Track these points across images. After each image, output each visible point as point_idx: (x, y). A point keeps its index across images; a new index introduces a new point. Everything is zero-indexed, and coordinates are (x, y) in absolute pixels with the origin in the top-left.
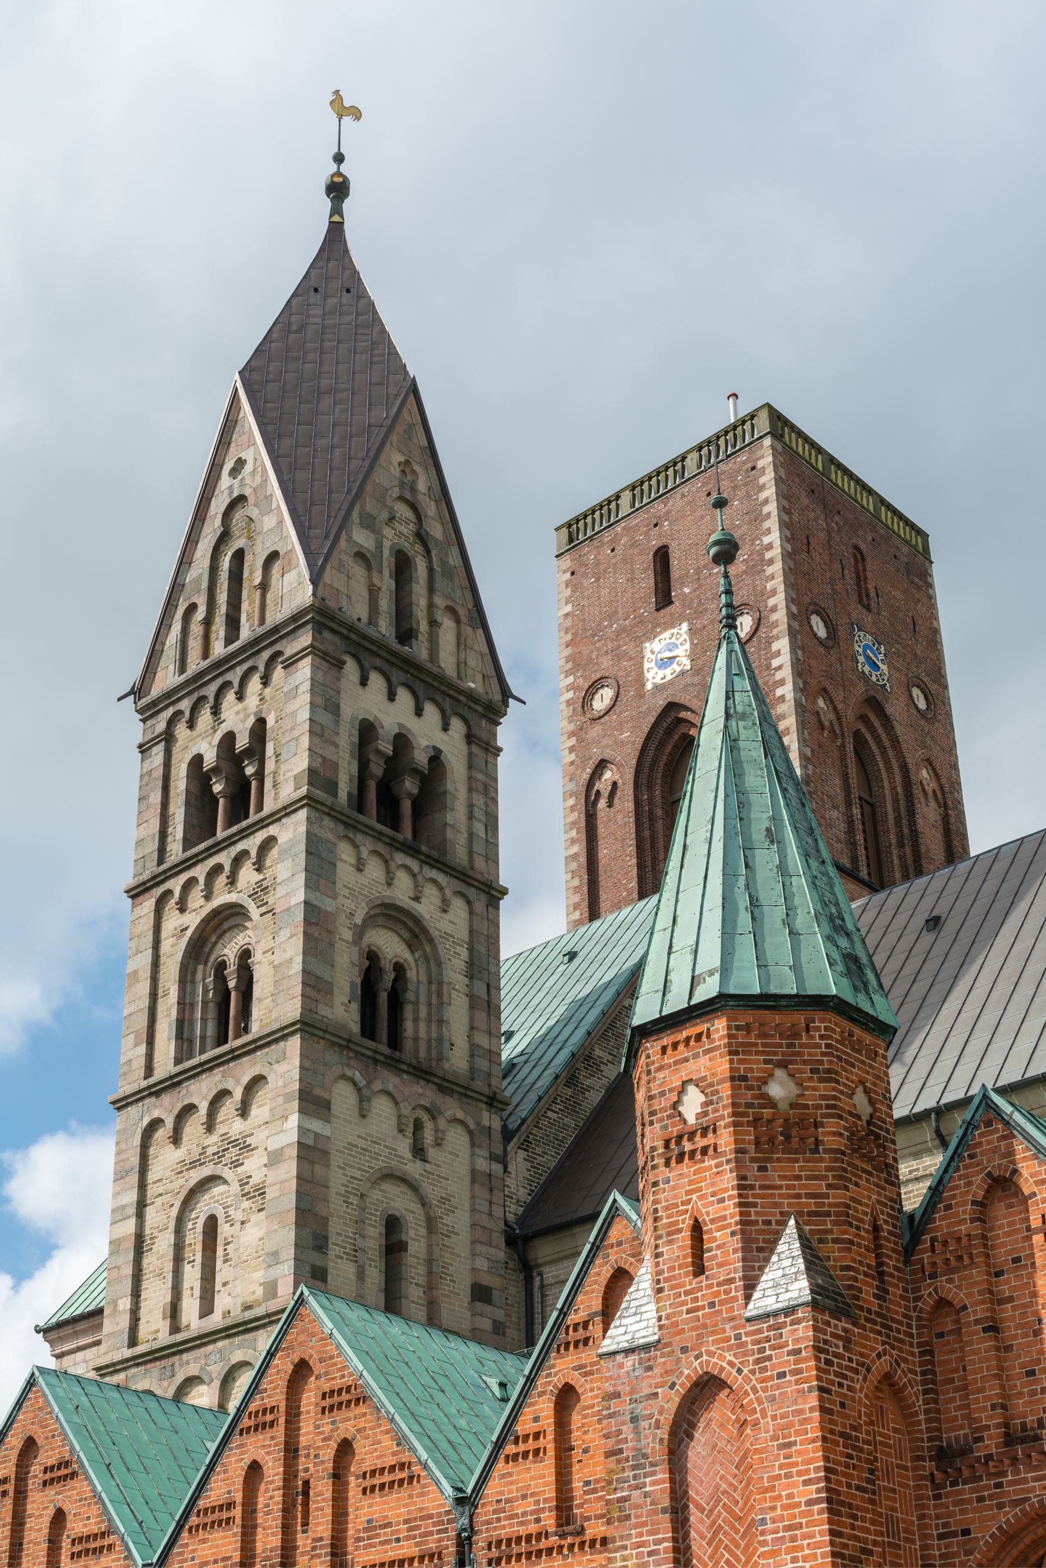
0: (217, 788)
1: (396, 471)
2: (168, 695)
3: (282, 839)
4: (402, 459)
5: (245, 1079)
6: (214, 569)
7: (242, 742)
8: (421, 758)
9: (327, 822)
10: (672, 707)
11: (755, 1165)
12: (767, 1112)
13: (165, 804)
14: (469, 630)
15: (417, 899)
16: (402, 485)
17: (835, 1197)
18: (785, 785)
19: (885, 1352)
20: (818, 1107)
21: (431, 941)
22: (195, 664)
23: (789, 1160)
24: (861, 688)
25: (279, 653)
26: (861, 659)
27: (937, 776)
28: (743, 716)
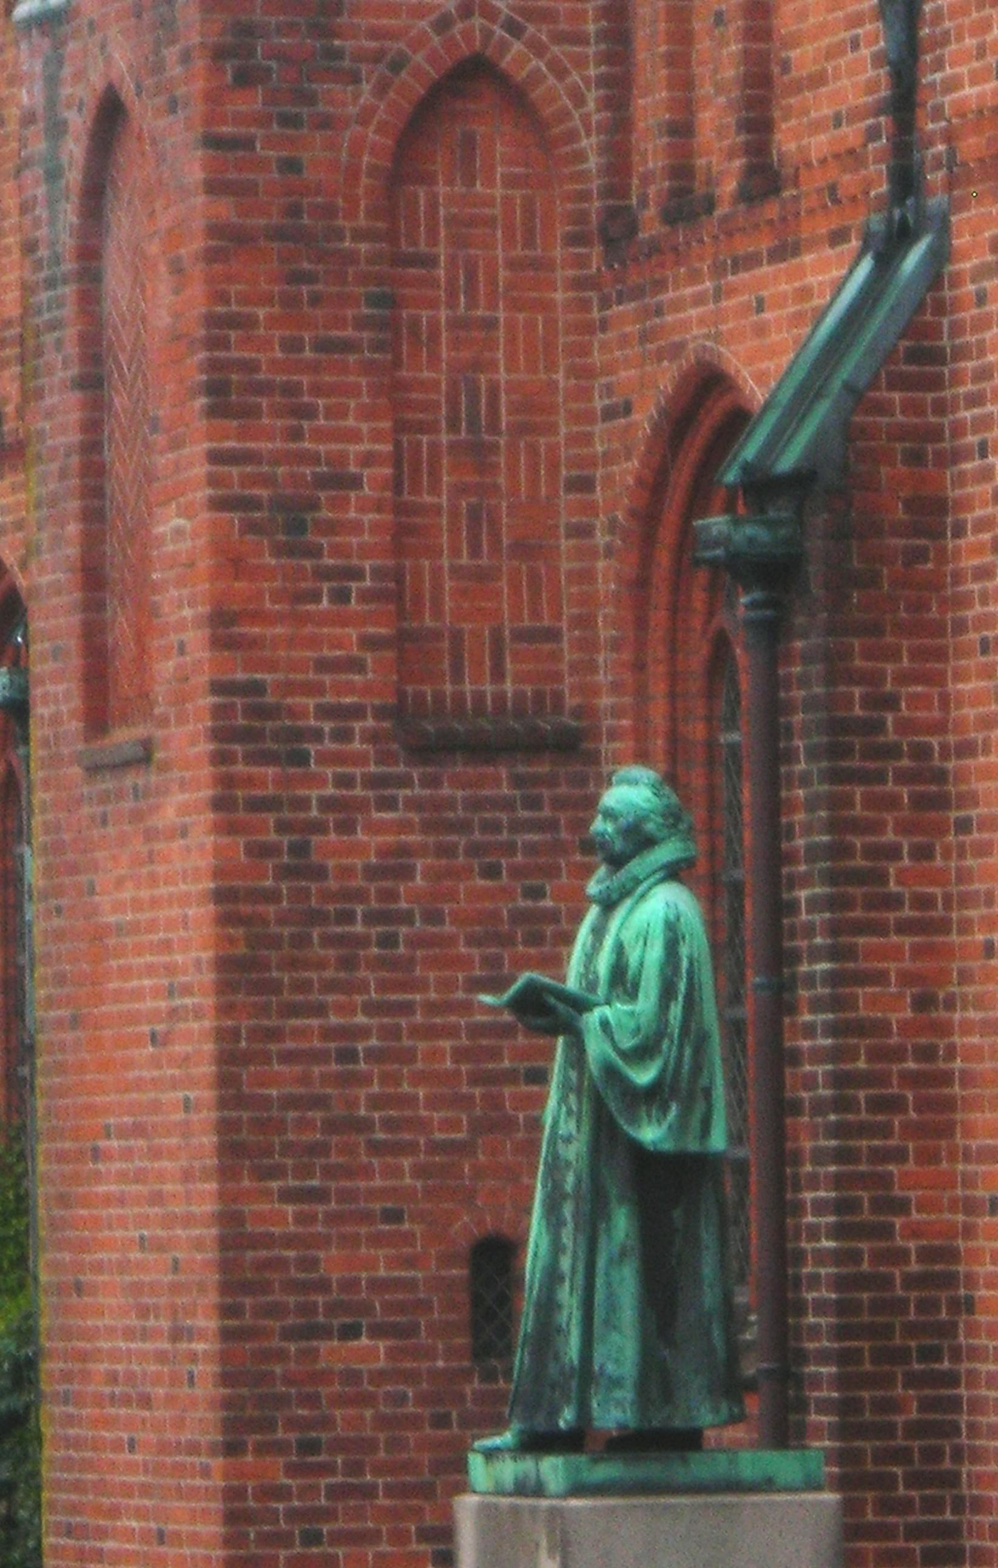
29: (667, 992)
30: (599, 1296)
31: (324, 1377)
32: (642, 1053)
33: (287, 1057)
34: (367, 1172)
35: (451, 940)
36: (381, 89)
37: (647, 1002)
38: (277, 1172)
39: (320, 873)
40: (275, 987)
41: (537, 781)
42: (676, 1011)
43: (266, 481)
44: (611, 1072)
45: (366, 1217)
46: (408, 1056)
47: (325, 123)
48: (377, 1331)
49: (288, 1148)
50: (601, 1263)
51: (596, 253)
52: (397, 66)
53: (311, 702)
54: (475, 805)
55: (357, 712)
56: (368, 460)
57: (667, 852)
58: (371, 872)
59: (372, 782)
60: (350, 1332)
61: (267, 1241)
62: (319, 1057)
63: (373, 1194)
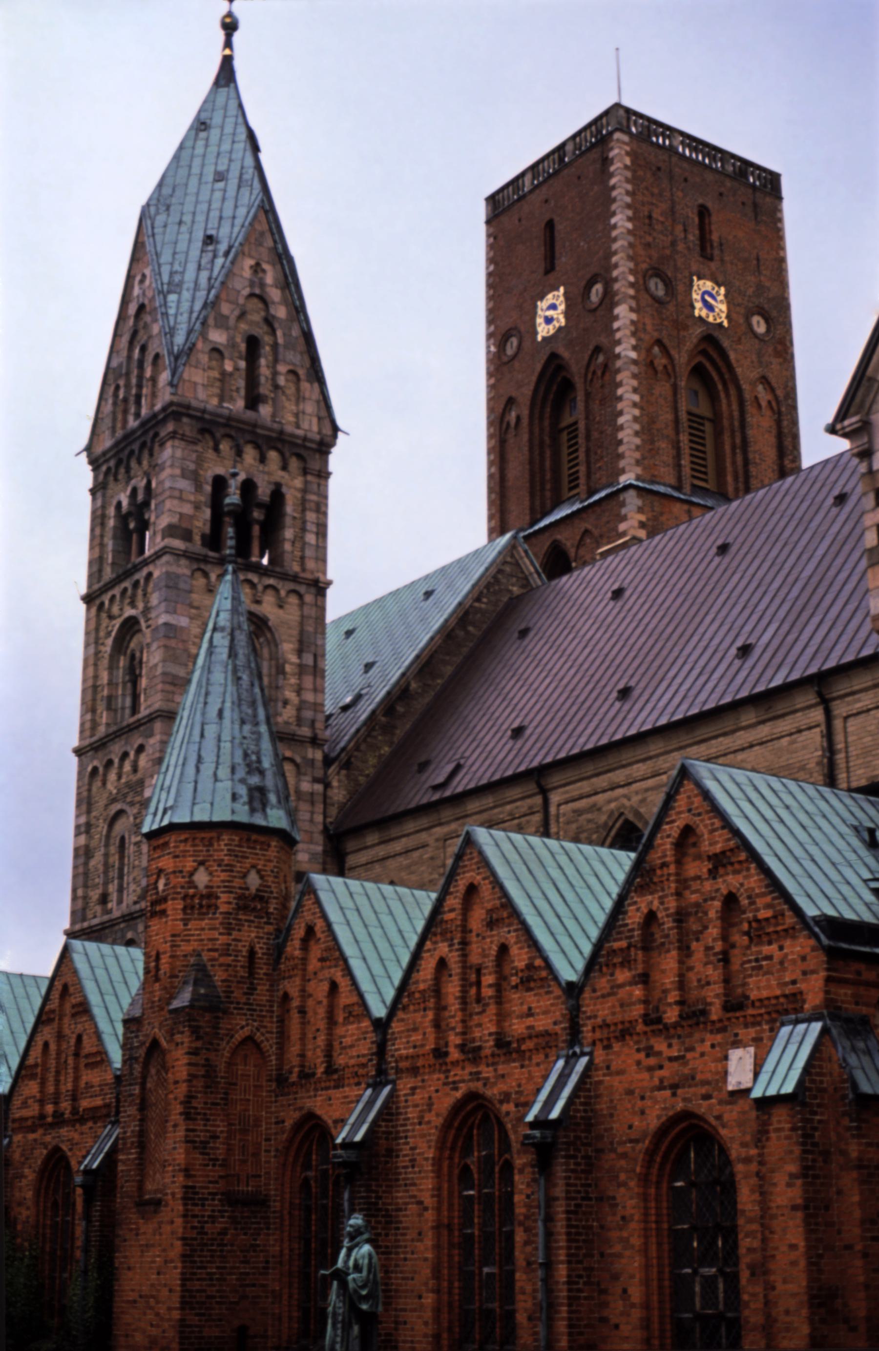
0: (132, 525)
1: (247, 273)
2: (104, 454)
3: (156, 574)
4: (252, 262)
5: (136, 746)
6: (129, 357)
7: (140, 497)
9: (183, 562)
10: (553, 356)
12: (191, 891)
13: (102, 536)
15: (258, 602)
16: (252, 284)
17: (223, 939)
18: (240, 674)
19: (247, 1025)
20: (219, 887)
21: (269, 629)
22: (119, 433)
24: (698, 331)
25: (156, 435)
26: (698, 305)
27: (772, 390)
28: (223, 629)
29: (369, 1271)
33: (198, 1280)
36: (228, 1043)
37: (365, 1273)
39: (206, 1233)
40: (195, 1262)
42: (371, 1276)
52: (232, 1037)
53: (206, 1191)
56: (222, 1132)
57: (366, 1236)
59: (219, 1211)
61: (190, 1326)
62: (204, 1279)
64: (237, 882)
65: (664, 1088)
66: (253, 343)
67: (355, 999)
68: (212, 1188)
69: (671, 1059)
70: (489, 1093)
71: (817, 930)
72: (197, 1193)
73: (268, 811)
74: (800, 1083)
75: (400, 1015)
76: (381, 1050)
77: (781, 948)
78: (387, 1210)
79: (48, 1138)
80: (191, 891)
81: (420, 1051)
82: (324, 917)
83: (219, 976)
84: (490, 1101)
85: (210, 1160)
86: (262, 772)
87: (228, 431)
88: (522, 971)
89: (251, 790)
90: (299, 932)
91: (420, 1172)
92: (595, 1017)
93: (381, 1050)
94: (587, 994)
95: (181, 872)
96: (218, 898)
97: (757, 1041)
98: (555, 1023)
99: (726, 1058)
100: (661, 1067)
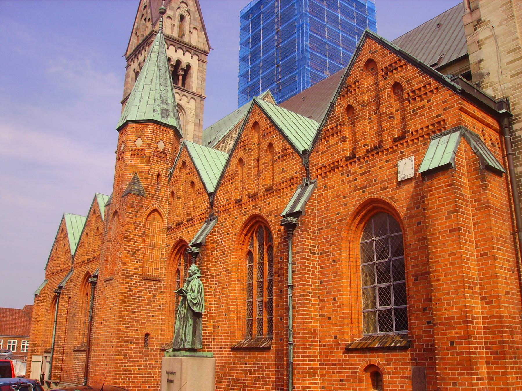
8: (183, 65)
11: (130, 161)
14: (200, 33)
15: (180, 100)
17: (147, 168)
19: (155, 204)
20: (146, 146)
21: (184, 110)
23: (137, 159)
29: (198, 292)
30: (187, 330)
31: (128, 347)
32: (195, 299)
33: (127, 311)
34: (134, 325)
35: (146, 300)
36: (146, 210)
37: (196, 292)
38: (125, 324)
39: (132, 291)
40: (126, 303)
41: (156, 284)
42: (199, 294)
43: (131, 249)
44: (191, 301)
45: (134, 330)
46: (140, 312)
47: (140, 213)
48: (134, 343)
49: (126, 321)
50: (187, 326)
51: (166, 230)
52: (148, 208)
54: (149, 286)
55: (138, 274)
56: (141, 248)
58: (138, 292)
59: (139, 282)
60: (131, 343)
61: (123, 332)
62: (130, 311)
63: (135, 327)
64: (154, 145)
65: (358, 190)
66: (182, 18)
67: (202, 186)
68: (136, 272)
69: (361, 174)
70: (262, 214)
71: (452, 83)
72: (129, 273)
73: (169, 118)
74: (453, 159)
75: (220, 188)
76: (212, 205)
77: (429, 101)
78: (211, 275)
79: (85, 269)
80: (134, 148)
81: (229, 202)
82: (190, 156)
83: (143, 182)
84: (262, 218)
85: (135, 259)
86: (167, 104)
87: (172, 43)
88: (279, 153)
89: (162, 109)
90: (179, 164)
91: (227, 256)
92: (318, 164)
93: (212, 205)
94: (313, 155)
95: (131, 140)
96: (145, 150)
97: (416, 152)
98: (296, 173)
99: (396, 166)
100: (356, 180)
